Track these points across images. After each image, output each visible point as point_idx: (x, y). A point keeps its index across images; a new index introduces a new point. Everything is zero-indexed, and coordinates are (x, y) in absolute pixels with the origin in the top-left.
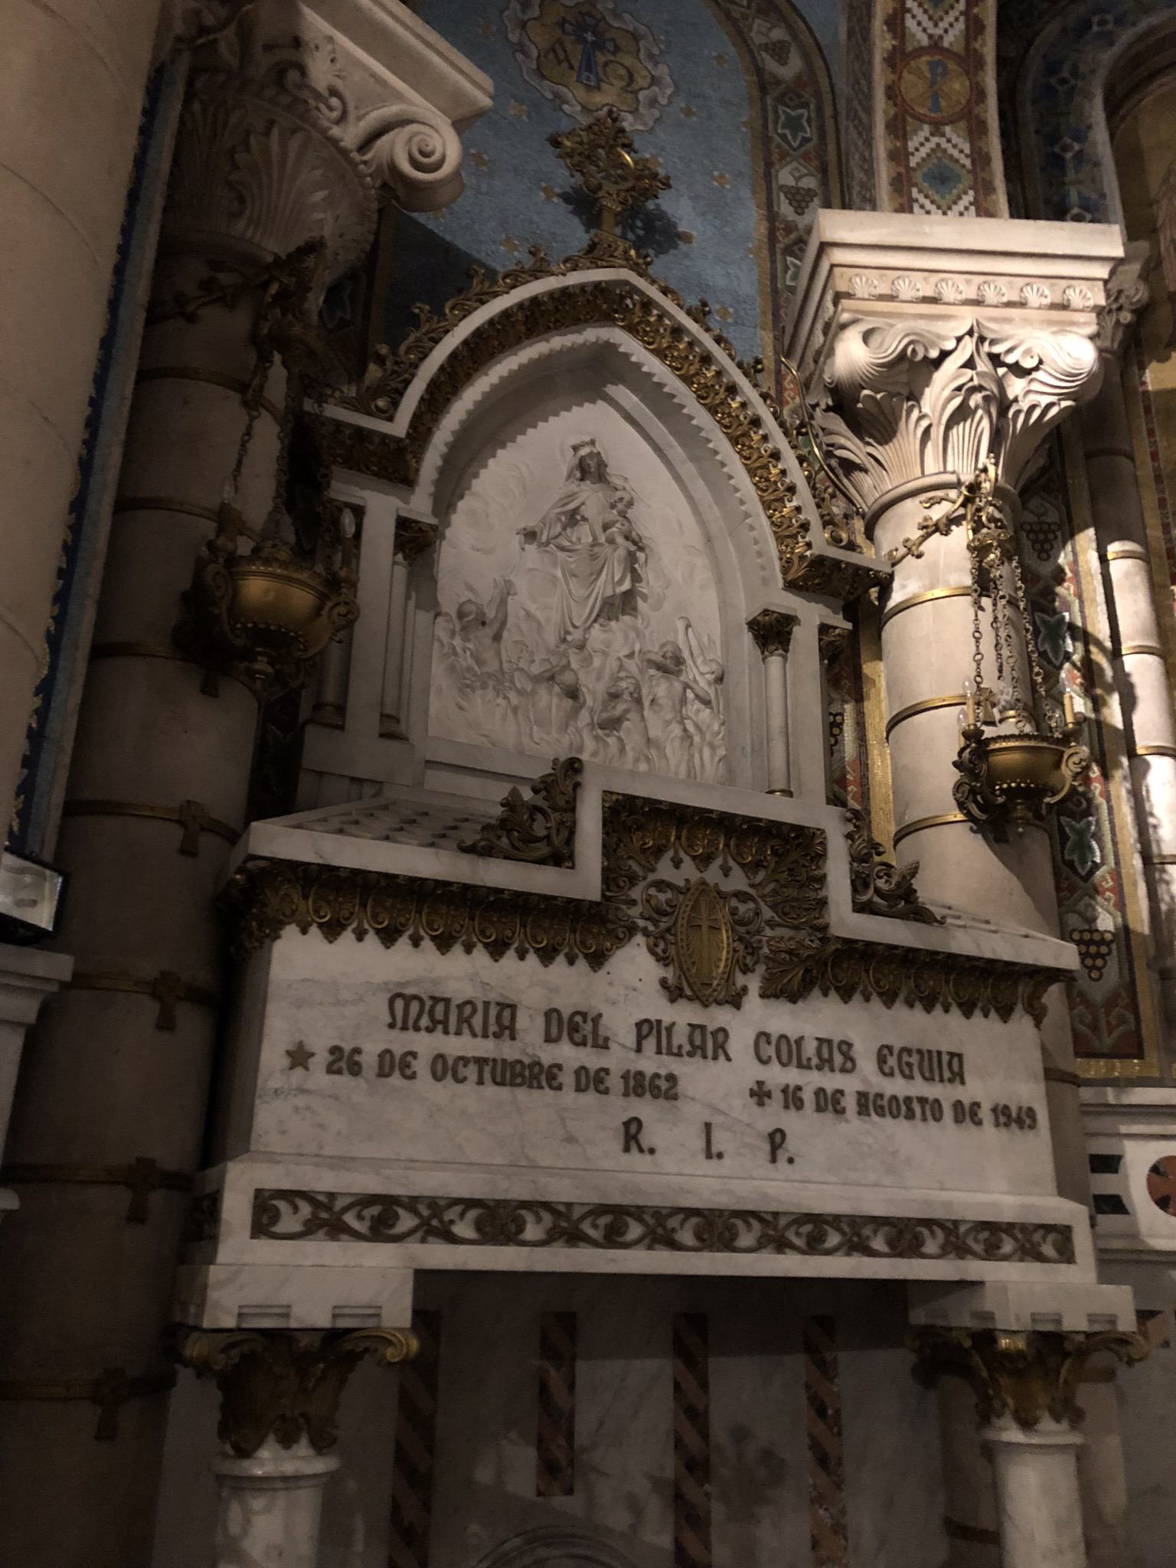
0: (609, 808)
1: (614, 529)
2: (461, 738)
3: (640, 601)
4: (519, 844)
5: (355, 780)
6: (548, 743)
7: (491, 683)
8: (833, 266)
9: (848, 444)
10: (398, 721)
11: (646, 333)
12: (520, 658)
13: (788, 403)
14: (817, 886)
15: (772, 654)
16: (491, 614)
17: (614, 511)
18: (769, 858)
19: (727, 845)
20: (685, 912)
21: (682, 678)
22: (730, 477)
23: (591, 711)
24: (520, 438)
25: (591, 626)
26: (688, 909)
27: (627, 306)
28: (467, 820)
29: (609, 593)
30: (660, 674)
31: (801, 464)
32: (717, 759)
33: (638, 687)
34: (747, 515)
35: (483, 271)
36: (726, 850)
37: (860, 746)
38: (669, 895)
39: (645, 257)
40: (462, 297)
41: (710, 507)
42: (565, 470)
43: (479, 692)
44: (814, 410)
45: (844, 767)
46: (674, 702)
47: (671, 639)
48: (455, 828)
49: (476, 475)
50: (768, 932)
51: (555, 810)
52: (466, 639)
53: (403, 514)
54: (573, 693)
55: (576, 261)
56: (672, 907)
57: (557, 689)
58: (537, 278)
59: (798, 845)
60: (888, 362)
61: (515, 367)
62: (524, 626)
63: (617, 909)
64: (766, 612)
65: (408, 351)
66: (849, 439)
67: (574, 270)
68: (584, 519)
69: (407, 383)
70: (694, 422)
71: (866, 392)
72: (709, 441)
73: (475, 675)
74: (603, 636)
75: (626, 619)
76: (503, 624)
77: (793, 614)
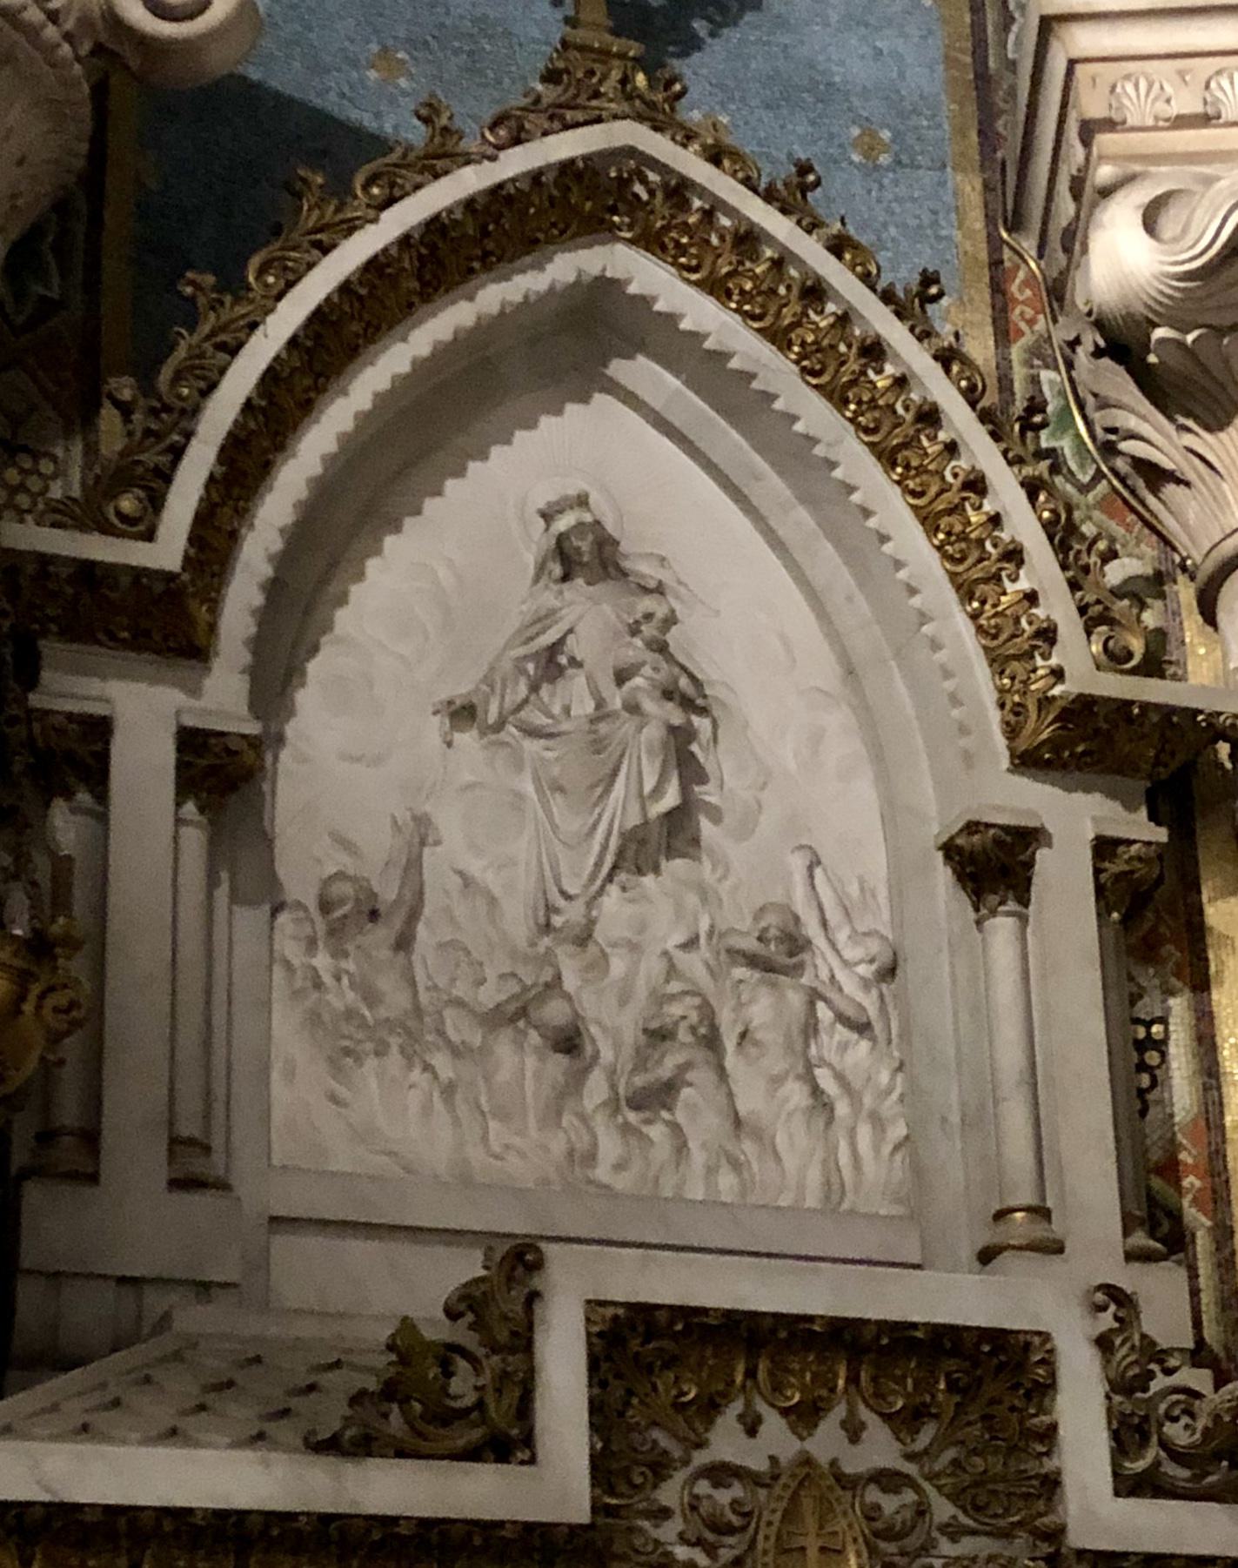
0: (600, 1335)
1: (638, 681)
2: (341, 1162)
3: (706, 826)
4: (420, 1425)
5: (122, 1280)
6: (522, 1154)
7: (395, 1042)
8: (1072, 63)
9: (1145, 429)
10: (207, 1149)
11: (682, 250)
12: (453, 980)
13: (1021, 333)
14: (1041, 1449)
15: (993, 913)
16: (388, 892)
17: (638, 642)
18: (940, 1397)
19: (853, 1379)
20: (770, 1524)
21: (804, 980)
22: (884, 539)
23: (612, 1073)
24: (431, 505)
25: (601, 891)
26: (778, 1515)
27: (636, 196)
28: (337, 1364)
29: (634, 820)
30: (757, 975)
31: (1032, 497)
32: (887, 1149)
33: (708, 1012)
34: (924, 617)
35: (320, 180)
36: (852, 1389)
37: (1206, 1088)
38: (737, 1490)
39: (669, 84)
40: (278, 245)
41: (849, 599)
42: (530, 560)
43: (371, 1063)
44: (1074, 351)
45: (1172, 1140)
46: (788, 1036)
47: (778, 896)
48: (312, 1388)
49: (342, 600)
50: (946, 1547)
51: (495, 1349)
52: (339, 953)
53: (189, 721)
54: (569, 1042)
55: (519, 118)
56: (748, 1515)
57: (534, 1037)
58: (436, 176)
59: (1001, 1367)
60: (1203, 267)
61: (404, 367)
62: (460, 911)
63: (631, 1530)
64: (972, 827)
65: (178, 377)
66: (1144, 418)
67: (517, 141)
68: (575, 663)
69: (178, 452)
70: (799, 427)
71: (1160, 333)
72: (833, 465)
73: (363, 1025)
74: (629, 909)
75: (676, 867)
76: (414, 915)
77: (1032, 823)
